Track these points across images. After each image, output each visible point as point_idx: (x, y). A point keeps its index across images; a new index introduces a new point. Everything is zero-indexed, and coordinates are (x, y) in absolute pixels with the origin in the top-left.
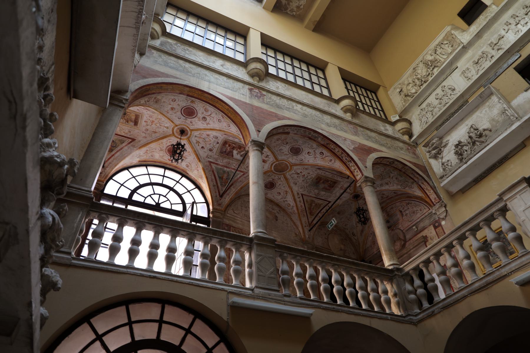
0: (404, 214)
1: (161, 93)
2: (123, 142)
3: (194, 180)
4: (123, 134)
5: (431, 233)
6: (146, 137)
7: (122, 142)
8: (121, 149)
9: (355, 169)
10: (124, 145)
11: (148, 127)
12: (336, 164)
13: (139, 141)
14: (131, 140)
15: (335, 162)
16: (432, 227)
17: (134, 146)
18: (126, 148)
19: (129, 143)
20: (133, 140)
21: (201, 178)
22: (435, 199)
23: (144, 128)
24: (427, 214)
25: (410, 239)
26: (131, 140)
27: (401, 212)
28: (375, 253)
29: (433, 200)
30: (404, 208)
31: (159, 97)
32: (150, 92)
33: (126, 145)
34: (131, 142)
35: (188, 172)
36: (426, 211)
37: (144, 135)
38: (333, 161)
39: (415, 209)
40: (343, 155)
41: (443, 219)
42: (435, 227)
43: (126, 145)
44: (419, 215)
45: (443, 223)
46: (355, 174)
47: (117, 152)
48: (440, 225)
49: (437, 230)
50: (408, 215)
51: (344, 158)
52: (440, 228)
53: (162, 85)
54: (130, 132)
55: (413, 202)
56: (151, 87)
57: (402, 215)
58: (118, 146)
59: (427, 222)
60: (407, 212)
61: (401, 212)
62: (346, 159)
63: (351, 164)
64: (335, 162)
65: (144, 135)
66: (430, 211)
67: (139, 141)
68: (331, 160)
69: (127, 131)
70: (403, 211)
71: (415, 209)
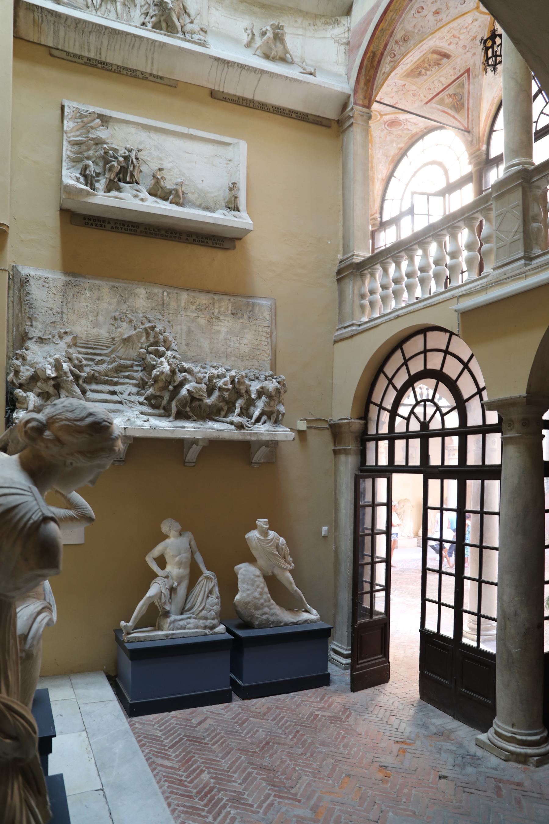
1: (392, 32)
2: (463, 85)
4: (453, 78)
6: (474, 54)
7: (462, 86)
8: (469, 93)
10: (466, 86)
11: (461, 43)
13: (475, 65)
14: (466, 75)
17: (476, 76)
18: (471, 87)
19: (469, 79)
20: (468, 71)
23: (460, 50)
26: (466, 75)
31: (399, 34)
32: (379, 53)
33: (469, 84)
34: (469, 76)
37: (469, 54)
43: (469, 84)
47: (468, 100)
53: (380, 27)
54: (455, 69)
56: (371, 48)
58: (463, 93)
65: (469, 54)
67: (475, 65)
69: (452, 72)
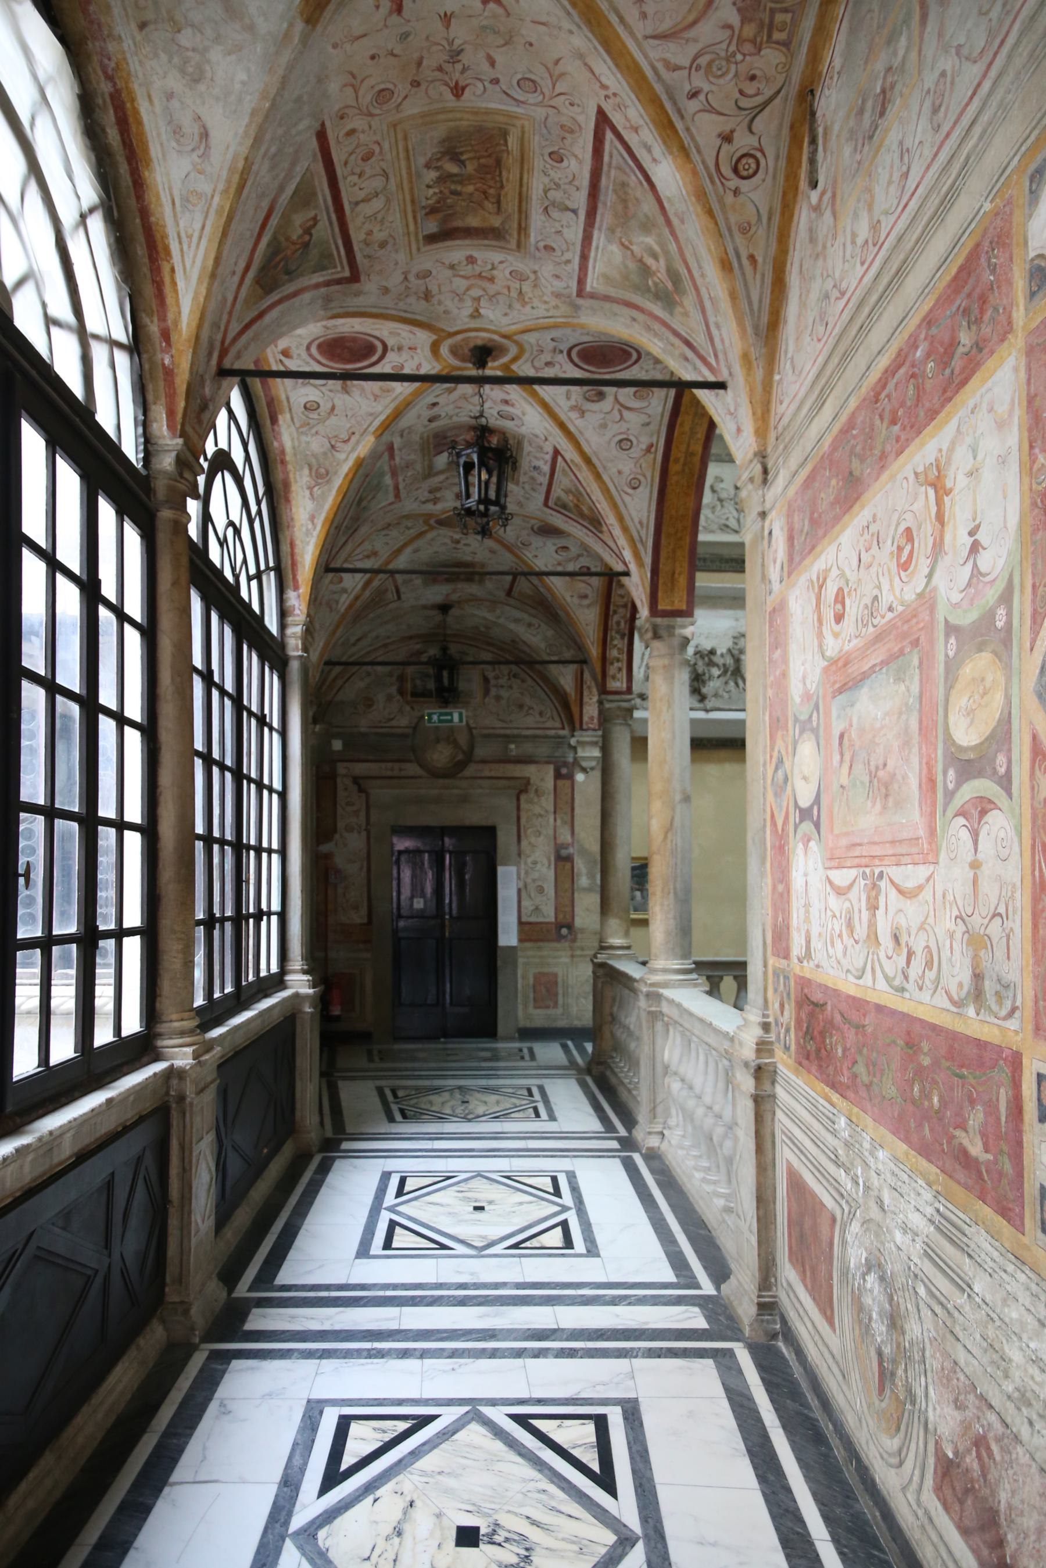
0: (493, 691)
3: (271, 456)
5: (542, 780)
9: (618, 660)
12: (586, 611)
15: (588, 606)
16: (551, 769)
21: (321, 475)
22: (592, 718)
24: (552, 732)
25: (484, 761)
27: (486, 680)
28: (363, 730)
29: (586, 719)
30: (497, 678)
35: (284, 420)
36: (554, 725)
38: (586, 602)
39: (528, 701)
40: (621, 611)
41: (584, 770)
42: (558, 776)
44: (530, 721)
45: (580, 777)
46: (612, 670)
48: (571, 777)
49: (560, 783)
50: (503, 702)
51: (616, 618)
52: (568, 783)
55: (529, 681)
57: (487, 692)
59: (543, 750)
60: (504, 693)
61: (486, 680)
62: (618, 623)
63: (619, 643)
64: (588, 606)
66: (562, 733)
68: (585, 597)
70: (493, 682)
71: (528, 701)
